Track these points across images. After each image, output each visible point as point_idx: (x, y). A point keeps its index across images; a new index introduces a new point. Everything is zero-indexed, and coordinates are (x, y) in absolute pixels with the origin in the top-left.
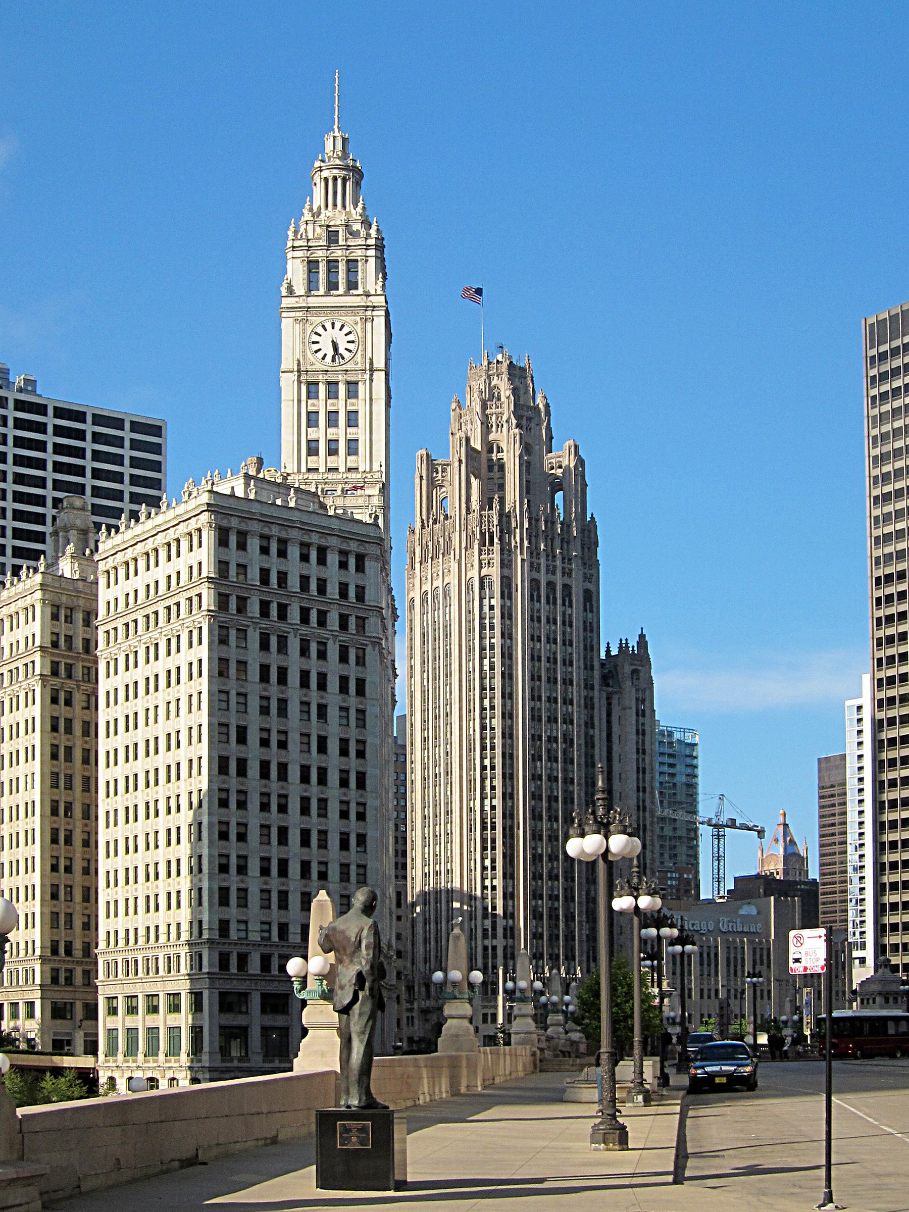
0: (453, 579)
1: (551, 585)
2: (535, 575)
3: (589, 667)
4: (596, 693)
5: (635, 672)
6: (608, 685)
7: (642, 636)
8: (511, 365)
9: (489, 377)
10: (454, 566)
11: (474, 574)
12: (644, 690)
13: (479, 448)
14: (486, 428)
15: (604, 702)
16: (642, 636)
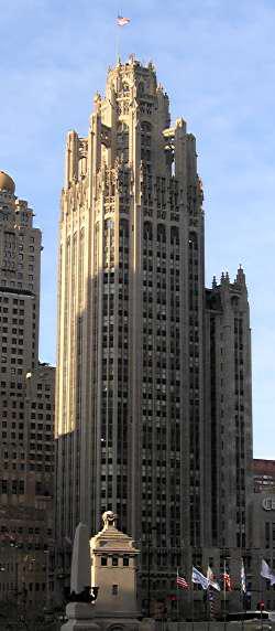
0: (85, 224)
1: (161, 227)
2: (148, 218)
3: (193, 293)
4: (200, 313)
5: (234, 298)
6: (211, 308)
7: (240, 271)
8: (137, 67)
9: (120, 75)
10: (86, 213)
11: (99, 218)
12: (241, 314)
13: (109, 125)
14: (117, 110)
15: (208, 323)
16: (240, 271)
